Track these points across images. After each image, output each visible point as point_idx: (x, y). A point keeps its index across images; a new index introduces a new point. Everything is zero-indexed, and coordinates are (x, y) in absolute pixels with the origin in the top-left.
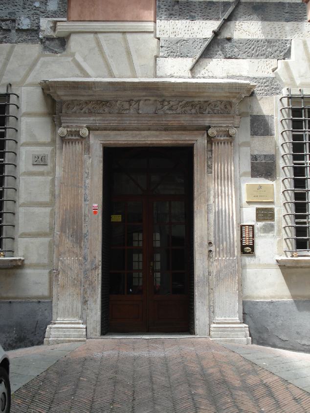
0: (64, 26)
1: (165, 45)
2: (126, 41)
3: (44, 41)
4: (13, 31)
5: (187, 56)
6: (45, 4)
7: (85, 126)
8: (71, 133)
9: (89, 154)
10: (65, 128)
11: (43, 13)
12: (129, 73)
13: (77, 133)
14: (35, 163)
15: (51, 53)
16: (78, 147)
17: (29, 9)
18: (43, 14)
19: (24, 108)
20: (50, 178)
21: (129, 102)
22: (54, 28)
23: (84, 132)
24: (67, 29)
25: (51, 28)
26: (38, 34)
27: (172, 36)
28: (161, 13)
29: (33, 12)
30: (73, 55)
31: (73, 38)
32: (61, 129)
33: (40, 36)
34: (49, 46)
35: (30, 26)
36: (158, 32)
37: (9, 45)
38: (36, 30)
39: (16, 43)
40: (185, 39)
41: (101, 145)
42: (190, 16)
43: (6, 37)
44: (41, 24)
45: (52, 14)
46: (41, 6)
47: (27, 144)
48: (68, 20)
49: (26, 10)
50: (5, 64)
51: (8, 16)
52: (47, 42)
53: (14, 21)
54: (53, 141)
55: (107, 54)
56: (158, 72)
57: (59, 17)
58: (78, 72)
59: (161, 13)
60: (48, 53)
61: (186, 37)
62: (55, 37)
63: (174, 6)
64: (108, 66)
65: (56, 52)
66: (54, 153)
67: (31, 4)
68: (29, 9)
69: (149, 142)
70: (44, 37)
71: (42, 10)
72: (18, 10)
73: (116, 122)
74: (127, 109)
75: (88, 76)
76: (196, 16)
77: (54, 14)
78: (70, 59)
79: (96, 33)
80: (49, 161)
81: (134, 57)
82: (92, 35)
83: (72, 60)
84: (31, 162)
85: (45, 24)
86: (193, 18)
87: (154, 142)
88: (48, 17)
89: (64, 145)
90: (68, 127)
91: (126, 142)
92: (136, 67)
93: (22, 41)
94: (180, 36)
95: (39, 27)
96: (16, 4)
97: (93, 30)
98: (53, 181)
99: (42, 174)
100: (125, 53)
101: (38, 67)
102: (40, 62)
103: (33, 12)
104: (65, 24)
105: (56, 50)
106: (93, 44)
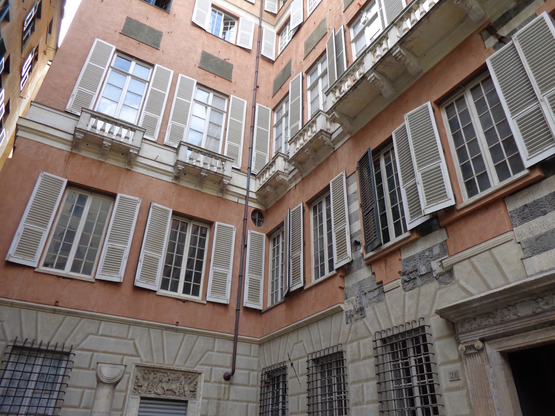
0: (447, 262)
1: (527, 246)
2: (492, 255)
3: (437, 278)
4: (418, 278)
5: (550, 248)
6: (432, 251)
7: (478, 339)
8: (468, 348)
9: (489, 364)
10: (462, 344)
11: (431, 258)
12: (503, 282)
13: (472, 347)
14: (451, 380)
15: (445, 285)
16: (478, 359)
17: (423, 259)
18: (432, 259)
19: (435, 335)
20: (465, 391)
21: (507, 308)
22: (442, 265)
23: (479, 344)
24: (449, 263)
25: (440, 266)
26: (432, 274)
27: (531, 236)
28: (514, 221)
29: (426, 260)
30: (457, 281)
31: (455, 268)
32: (460, 346)
33: (434, 275)
34: (442, 280)
35: (426, 271)
36: (517, 238)
37: (417, 288)
38: (430, 272)
39: (421, 286)
40: (543, 234)
41: (499, 353)
42: (542, 212)
43: (415, 284)
44: (432, 267)
45: (437, 256)
46: (430, 254)
47: (443, 364)
48: (450, 256)
49: (422, 260)
50: (418, 304)
51: (413, 269)
52: (441, 278)
53: (416, 270)
54: (460, 357)
55: (482, 273)
56: (527, 272)
57: (442, 257)
58: (464, 294)
59: (514, 221)
60: (443, 285)
61: (544, 231)
62: (444, 272)
63: (524, 210)
64: (485, 281)
65: (448, 283)
66: (462, 366)
67: (423, 254)
68: (423, 259)
69: (540, 341)
70: (437, 275)
71: (431, 256)
72: (417, 262)
73: (502, 329)
74: (508, 315)
75: (472, 295)
76: (546, 209)
77: (439, 256)
78: (456, 286)
79: (469, 258)
80: (461, 377)
81: (504, 267)
82: (467, 261)
83: (458, 286)
84: (448, 380)
85: (435, 265)
86: (545, 213)
87: (545, 340)
88: (435, 260)
89: (467, 360)
90: (465, 343)
91: (518, 346)
92: (507, 275)
93: (424, 283)
94: (538, 233)
95: (431, 269)
96: (415, 259)
97: (467, 257)
98: (468, 393)
99: (458, 389)
100: (495, 266)
101: (437, 299)
102: (437, 295)
103: (426, 260)
104: (447, 260)
105: (448, 281)
106: (470, 268)
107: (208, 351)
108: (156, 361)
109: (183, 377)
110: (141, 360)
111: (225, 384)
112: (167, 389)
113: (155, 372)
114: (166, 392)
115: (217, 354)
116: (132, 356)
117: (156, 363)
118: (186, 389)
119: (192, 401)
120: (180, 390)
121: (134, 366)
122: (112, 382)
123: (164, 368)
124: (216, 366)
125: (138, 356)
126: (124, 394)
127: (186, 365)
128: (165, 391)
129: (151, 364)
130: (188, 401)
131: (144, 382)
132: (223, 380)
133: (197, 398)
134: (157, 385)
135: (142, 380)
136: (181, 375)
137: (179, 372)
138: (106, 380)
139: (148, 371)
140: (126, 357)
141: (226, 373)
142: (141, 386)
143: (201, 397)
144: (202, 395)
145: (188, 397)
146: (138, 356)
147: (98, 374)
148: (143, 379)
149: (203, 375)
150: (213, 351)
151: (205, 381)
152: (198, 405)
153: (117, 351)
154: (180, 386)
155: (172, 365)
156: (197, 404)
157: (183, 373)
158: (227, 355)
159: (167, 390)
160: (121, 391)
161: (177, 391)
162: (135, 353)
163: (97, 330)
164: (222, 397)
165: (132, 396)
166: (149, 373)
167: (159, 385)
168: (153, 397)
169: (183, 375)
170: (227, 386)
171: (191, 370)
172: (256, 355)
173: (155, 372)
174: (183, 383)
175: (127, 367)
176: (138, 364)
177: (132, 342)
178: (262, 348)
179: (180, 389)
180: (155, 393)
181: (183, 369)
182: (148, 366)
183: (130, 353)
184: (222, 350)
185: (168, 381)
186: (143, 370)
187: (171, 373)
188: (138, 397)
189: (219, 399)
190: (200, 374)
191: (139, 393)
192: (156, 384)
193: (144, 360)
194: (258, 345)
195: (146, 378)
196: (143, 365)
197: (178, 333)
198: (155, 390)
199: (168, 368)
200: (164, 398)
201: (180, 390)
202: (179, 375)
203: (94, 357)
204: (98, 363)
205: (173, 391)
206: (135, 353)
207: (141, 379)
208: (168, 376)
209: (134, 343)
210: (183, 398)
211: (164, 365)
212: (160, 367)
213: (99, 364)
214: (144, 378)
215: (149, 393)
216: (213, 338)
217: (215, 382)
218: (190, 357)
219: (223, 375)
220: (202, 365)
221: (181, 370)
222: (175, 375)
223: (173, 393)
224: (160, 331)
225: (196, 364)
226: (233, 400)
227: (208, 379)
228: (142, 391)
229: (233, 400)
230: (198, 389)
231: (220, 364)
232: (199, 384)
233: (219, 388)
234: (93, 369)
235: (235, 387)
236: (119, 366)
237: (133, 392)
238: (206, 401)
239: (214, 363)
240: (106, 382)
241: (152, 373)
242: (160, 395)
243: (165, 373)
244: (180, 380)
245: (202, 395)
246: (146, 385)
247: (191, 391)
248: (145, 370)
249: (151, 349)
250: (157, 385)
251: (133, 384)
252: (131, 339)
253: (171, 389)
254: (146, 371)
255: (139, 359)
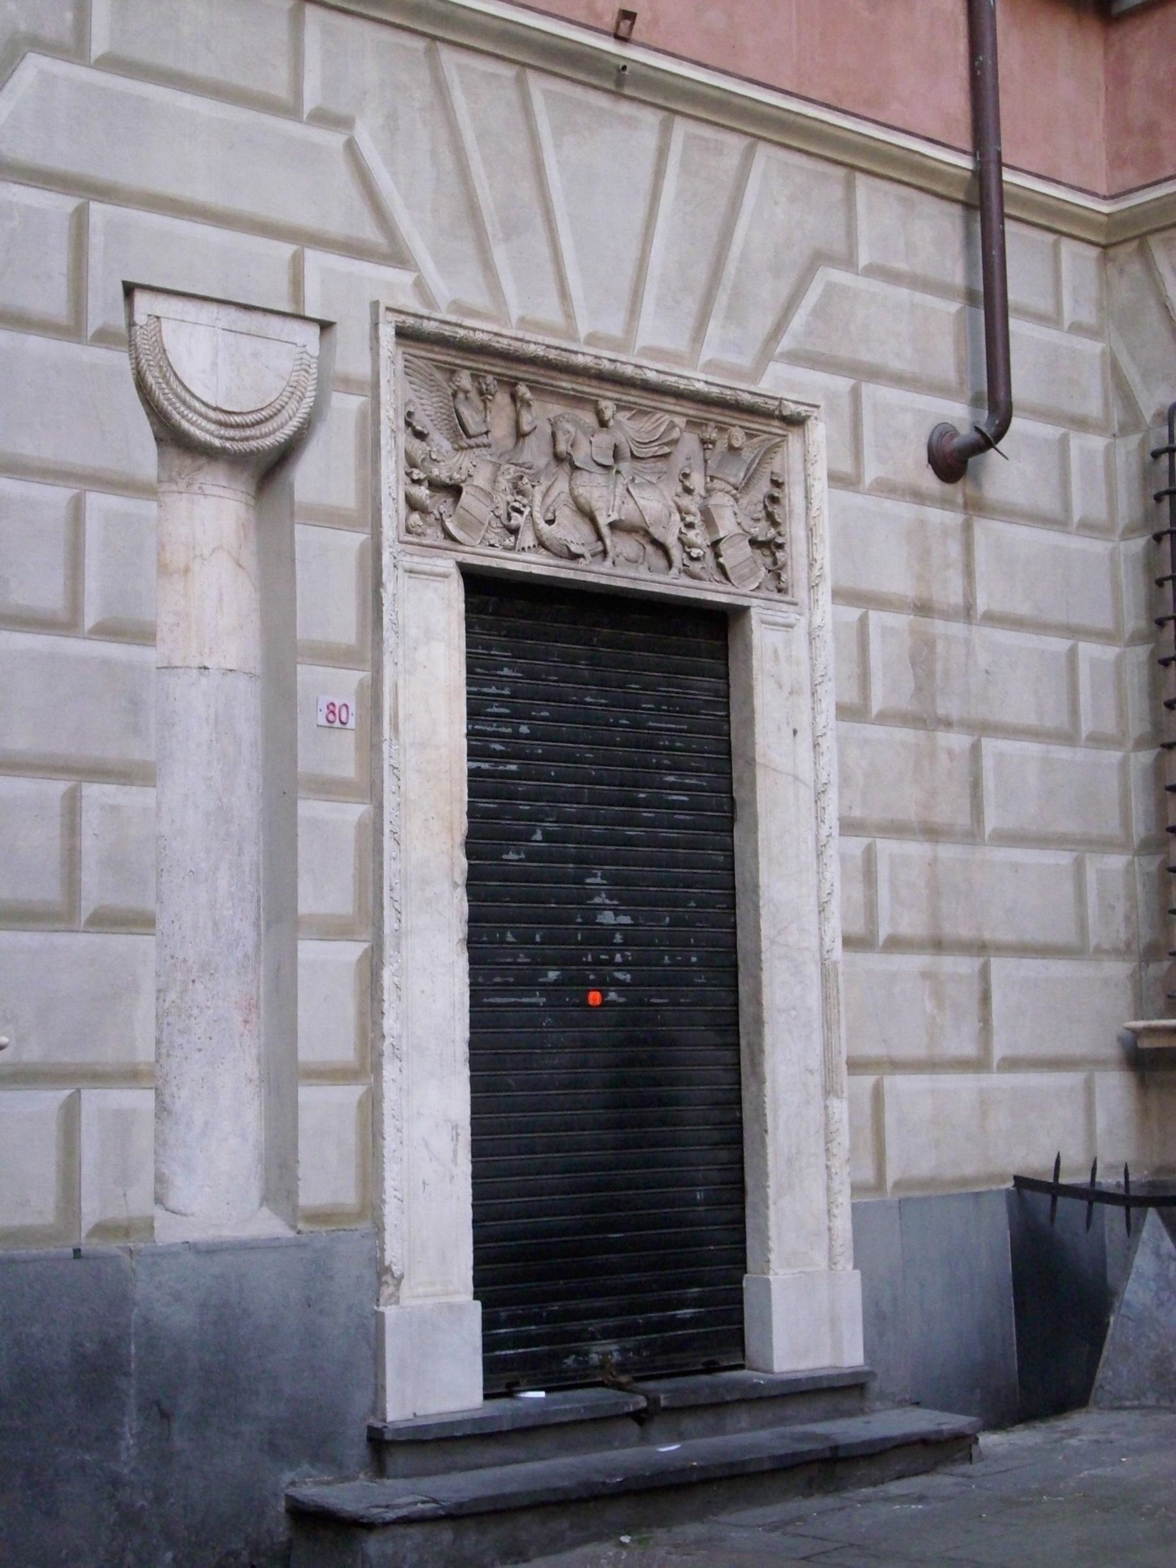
107: (819, 258)
108: (515, 312)
109: (690, 442)
110: (420, 285)
111: (945, 503)
112: (614, 517)
113: (523, 389)
114: (608, 542)
115: (875, 286)
116: (354, 249)
117: (522, 320)
118: (727, 525)
119: (770, 616)
120: (691, 535)
121: (387, 333)
122: (254, 444)
123: (580, 360)
124: (876, 374)
125: (397, 257)
126: (356, 539)
127: (707, 353)
128: (605, 531)
129: (495, 328)
130: (743, 611)
131: (465, 461)
132: (929, 481)
133: (800, 593)
134: (549, 489)
135: (446, 445)
136: (680, 421)
137: (670, 404)
138: (212, 427)
139: (476, 376)
140: (316, 261)
141: (944, 432)
142: (455, 491)
143: (824, 594)
144: (827, 569)
145: (743, 579)
146: (397, 257)
147: (150, 380)
148: (454, 438)
149: (818, 431)
150: (848, 262)
151: (835, 479)
152: (811, 638)
153: (246, 204)
154: (686, 501)
155: (623, 345)
156: (800, 632)
157: (691, 410)
158: (930, 300)
159: (613, 526)
160: (332, 518)
161: (671, 541)
162: (370, 233)
163: (69, 16)
164: (951, 593)
165: (407, 562)
166: (481, 393)
167: (554, 493)
168: (536, 570)
169: (693, 424)
170: (953, 518)
171: (744, 389)
172: (1088, 316)
173: (523, 389)
174: (697, 481)
175: (339, 331)
176: (410, 321)
177: (334, 140)
178: (1136, 268)
179: (690, 526)
180: (541, 544)
181: (698, 380)
182: (480, 336)
183: (336, 226)
184: (900, 265)
185: (609, 461)
186: (441, 366)
187: (620, 408)
188: (447, 564)
189: (923, 608)
190: (796, 422)
191: (449, 536)
192: (545, 483)
193: (443, 289)
194: (1094, 252)
195: (473, 428)
196: (447, 331)
197: (625, 108)
198: (543, 525)
199: (606, 366)
200: (604, 581)
201: (691, 535)
202: (672, 426)
203: (96, 239)
204: (129, 290)
205: (647, 533)
206: (370, 233)
207: (440, 442)
208: (603, 424)
209: (351, 147)
210: (714, 593)
211: (574, 339)
212: (552, 355)
213: (142, 300)
214: (460, 431)
215: (510, 541)
216: (841, 172)
217: (886, 488)
218: (722, 299)
219: (924, 440)
220: (796, 358)
221: (682, 384)
222: (646, 424)
223: (650, 548)
224: (507, 72)
225: (766, 355)
226: (994, 619)
227: (845, 466)
228: (462, 526)
229: (994, 619)
230: (795, 531)
231: (897, 365)
232: (794, 496)
233: (918, 532)
234: (104, 337)
235: (996, 526)
236: (276, 321)
237: (408, 531)
238: (852, 614)
239: (866, 356)
240: (217, 442)
241: (502, 399)
242: (575, 557)
243: (578, 400)
244: (678, 463)
245: (827, 569)
246: (482, 479)
247: (754, 543)
248: (451, 372)
249: (473, 211)
250: (549, 489)
251: (402, 472)
252: (322, 118)
253: (635, 519)
254: (465, 380)
255: (405, 278)
